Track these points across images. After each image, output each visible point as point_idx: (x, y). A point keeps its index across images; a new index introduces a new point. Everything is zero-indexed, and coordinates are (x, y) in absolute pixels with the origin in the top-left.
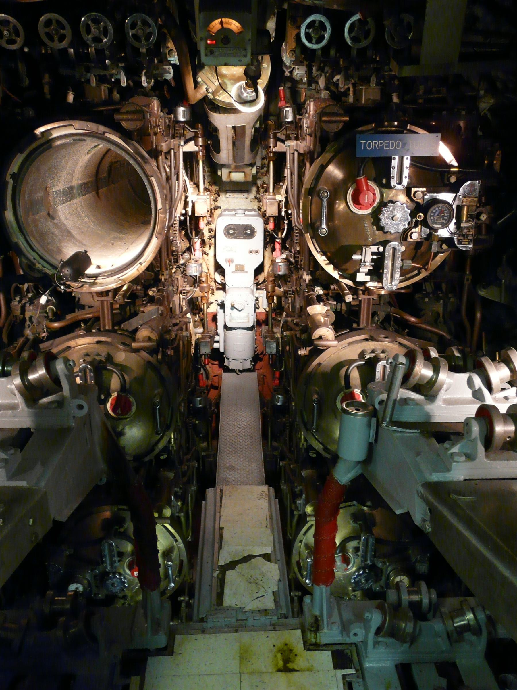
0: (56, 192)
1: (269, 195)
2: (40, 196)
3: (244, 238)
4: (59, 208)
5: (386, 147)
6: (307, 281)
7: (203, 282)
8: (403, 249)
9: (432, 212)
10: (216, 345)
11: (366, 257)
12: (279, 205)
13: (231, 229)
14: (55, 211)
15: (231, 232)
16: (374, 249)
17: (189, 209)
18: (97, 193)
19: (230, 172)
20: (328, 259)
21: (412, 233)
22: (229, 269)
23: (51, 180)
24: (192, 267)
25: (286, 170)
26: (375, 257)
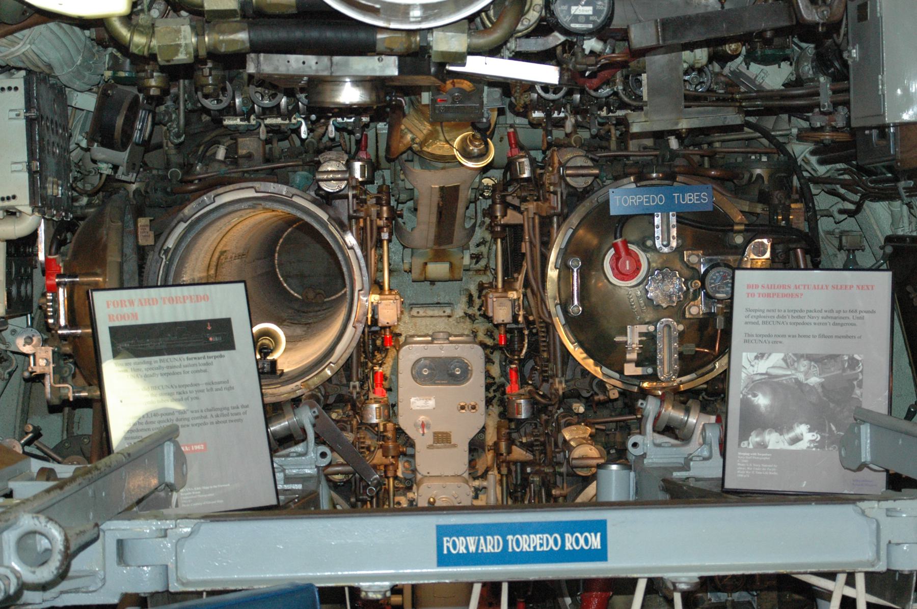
1: (496, 292)
3: (449, 384)
5: (648, 202)
6: (561, 392)
7: (388, 439)
8: (681, 327)
9: (712, 279)
11: (633, 338)
12: (513, 307)
13: (425, 366)
16: (643, 328)
19: (426, 264)
20: (586, 351)
21: (690, 308)
22: (422, 440)
25: (523, 244)
26: (644, 338)
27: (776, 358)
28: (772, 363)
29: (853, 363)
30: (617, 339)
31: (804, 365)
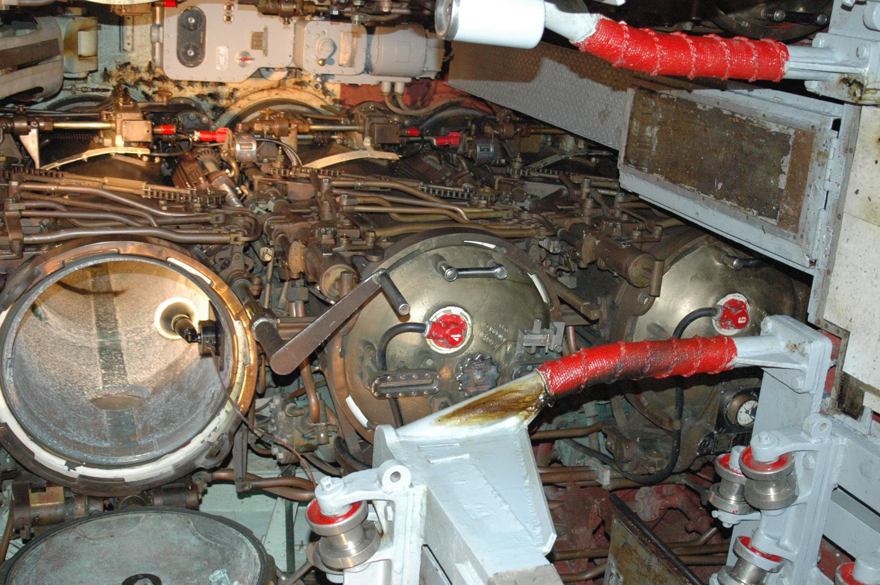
0: (105, 382)
2: (107, 417)
3: (204, 30)
4: (130, 379)
10: (399, 89)
14: (136, 387)
15: (192, 54)
17: (140, 151)
18: (116, 294)
19: (81, 57)
22: (259, 60)
23: (84, 394)
24: (241, 153)
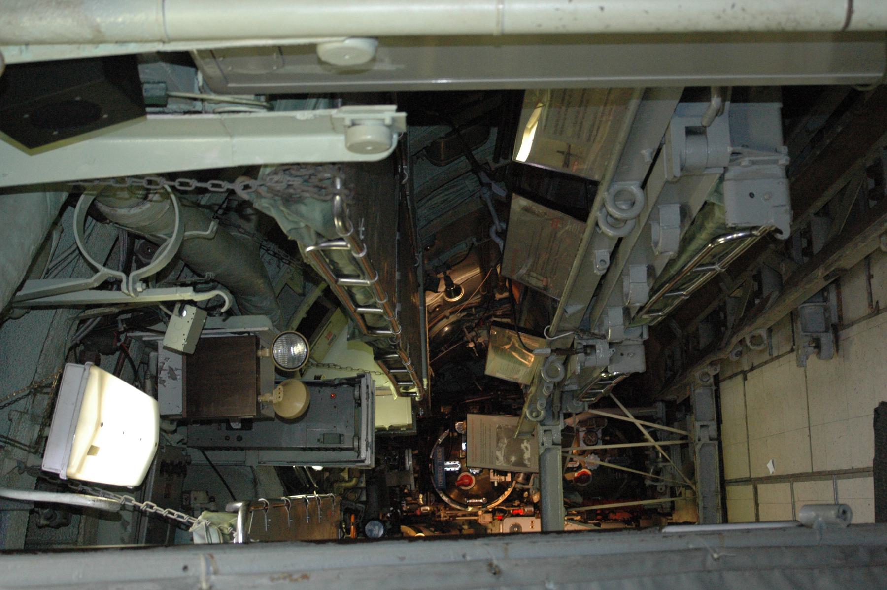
16: (492, 474)
27: (498, 454)
28: (500, 455)
29: (499, 427)
30: (496, 484)
31: (500, 444)
